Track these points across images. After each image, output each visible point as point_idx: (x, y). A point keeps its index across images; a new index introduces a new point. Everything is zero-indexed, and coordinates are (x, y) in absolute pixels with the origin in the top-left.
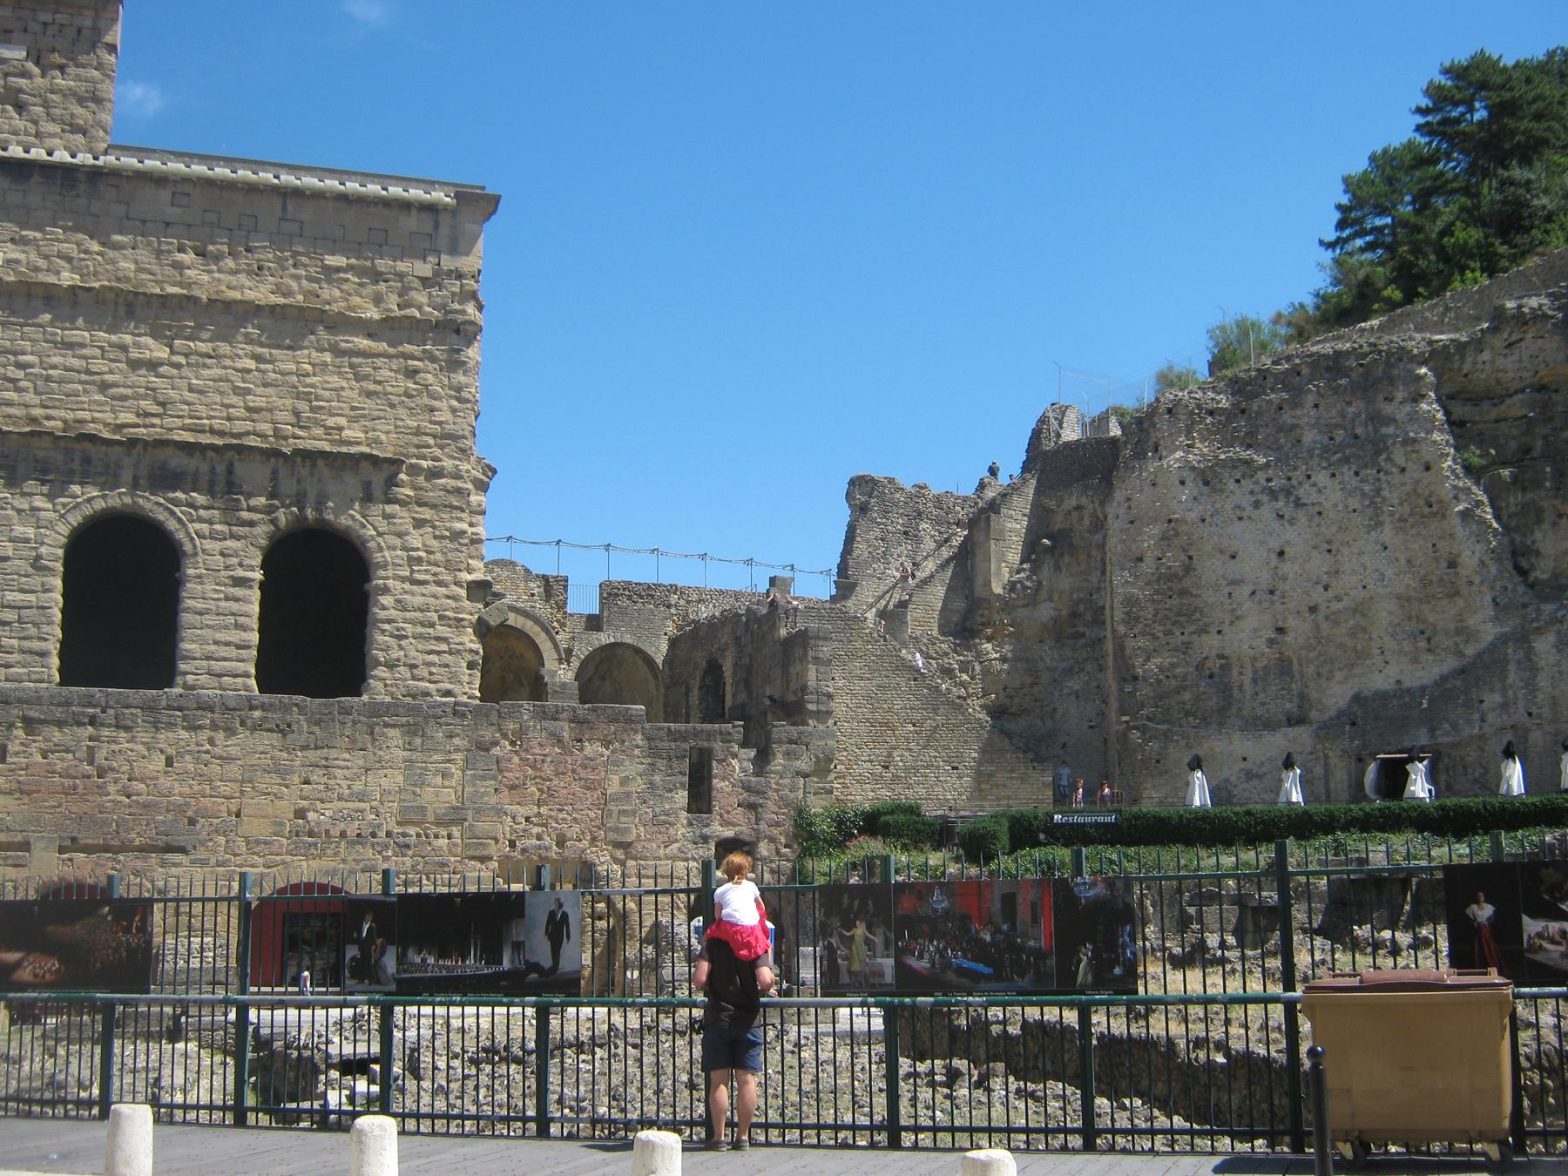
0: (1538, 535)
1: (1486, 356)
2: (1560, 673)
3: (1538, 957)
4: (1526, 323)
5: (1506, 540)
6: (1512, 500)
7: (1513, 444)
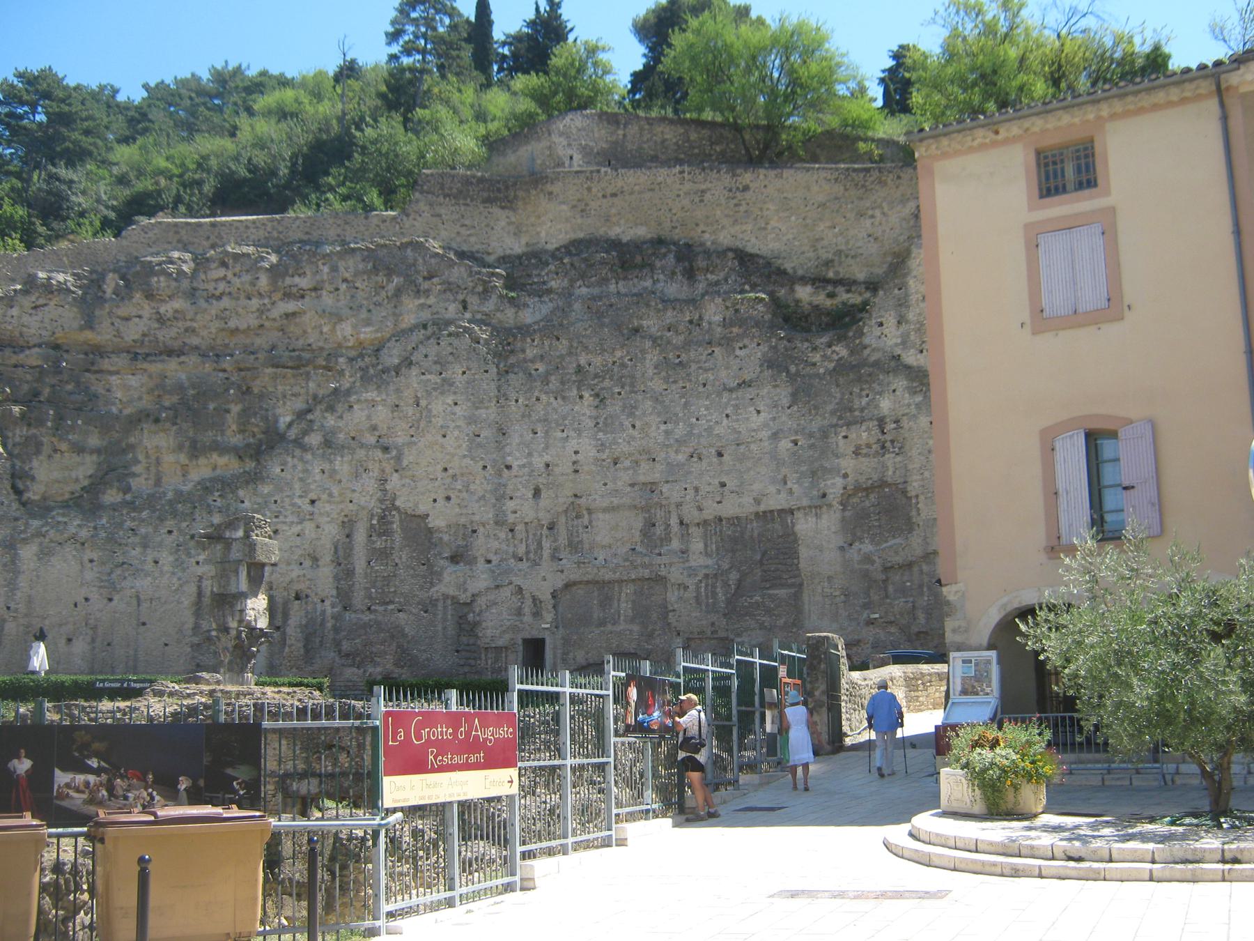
0: (35, 463)
1: (15, 311)
2: (38, 577)
3: (65, 803)
4: (52, 292)
5: (8, 465)
6: (18, 432)
7: (26, 387)
